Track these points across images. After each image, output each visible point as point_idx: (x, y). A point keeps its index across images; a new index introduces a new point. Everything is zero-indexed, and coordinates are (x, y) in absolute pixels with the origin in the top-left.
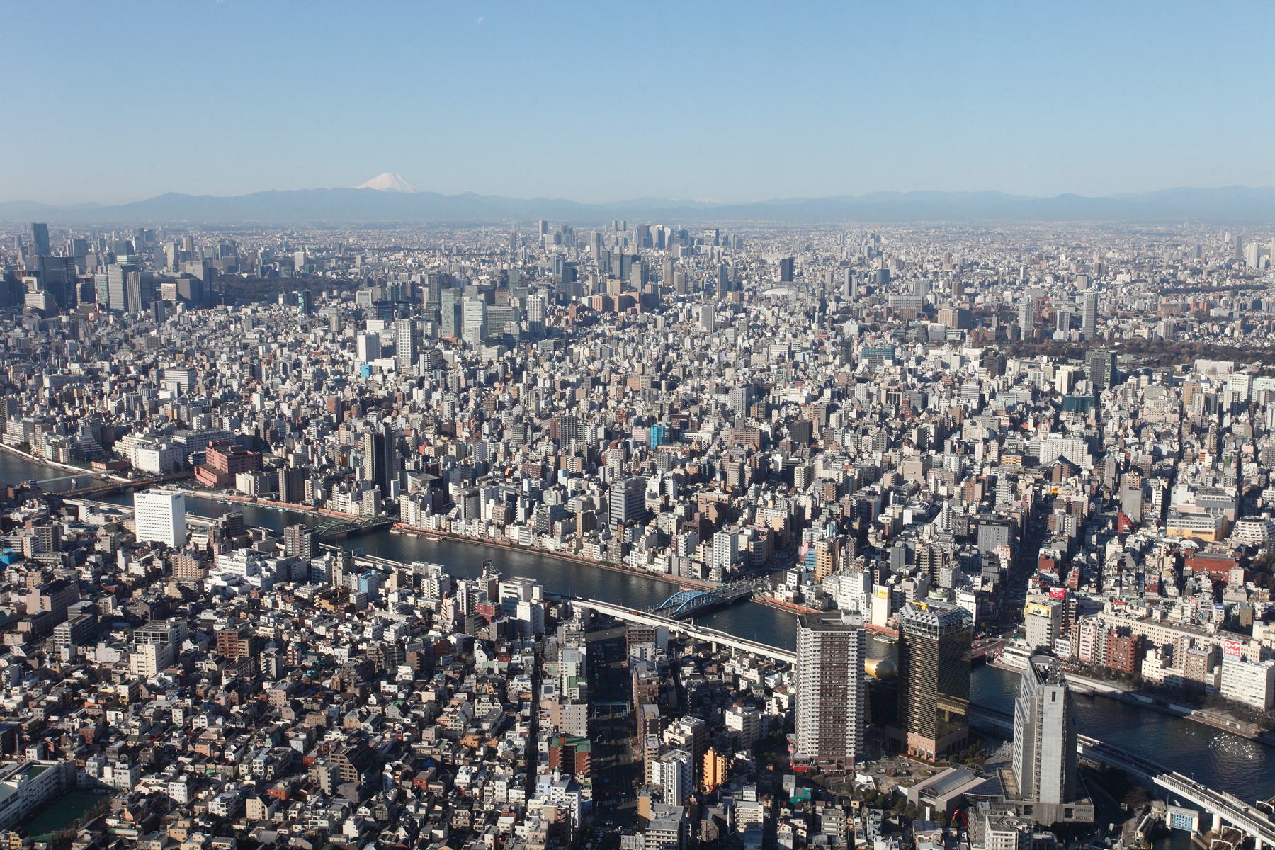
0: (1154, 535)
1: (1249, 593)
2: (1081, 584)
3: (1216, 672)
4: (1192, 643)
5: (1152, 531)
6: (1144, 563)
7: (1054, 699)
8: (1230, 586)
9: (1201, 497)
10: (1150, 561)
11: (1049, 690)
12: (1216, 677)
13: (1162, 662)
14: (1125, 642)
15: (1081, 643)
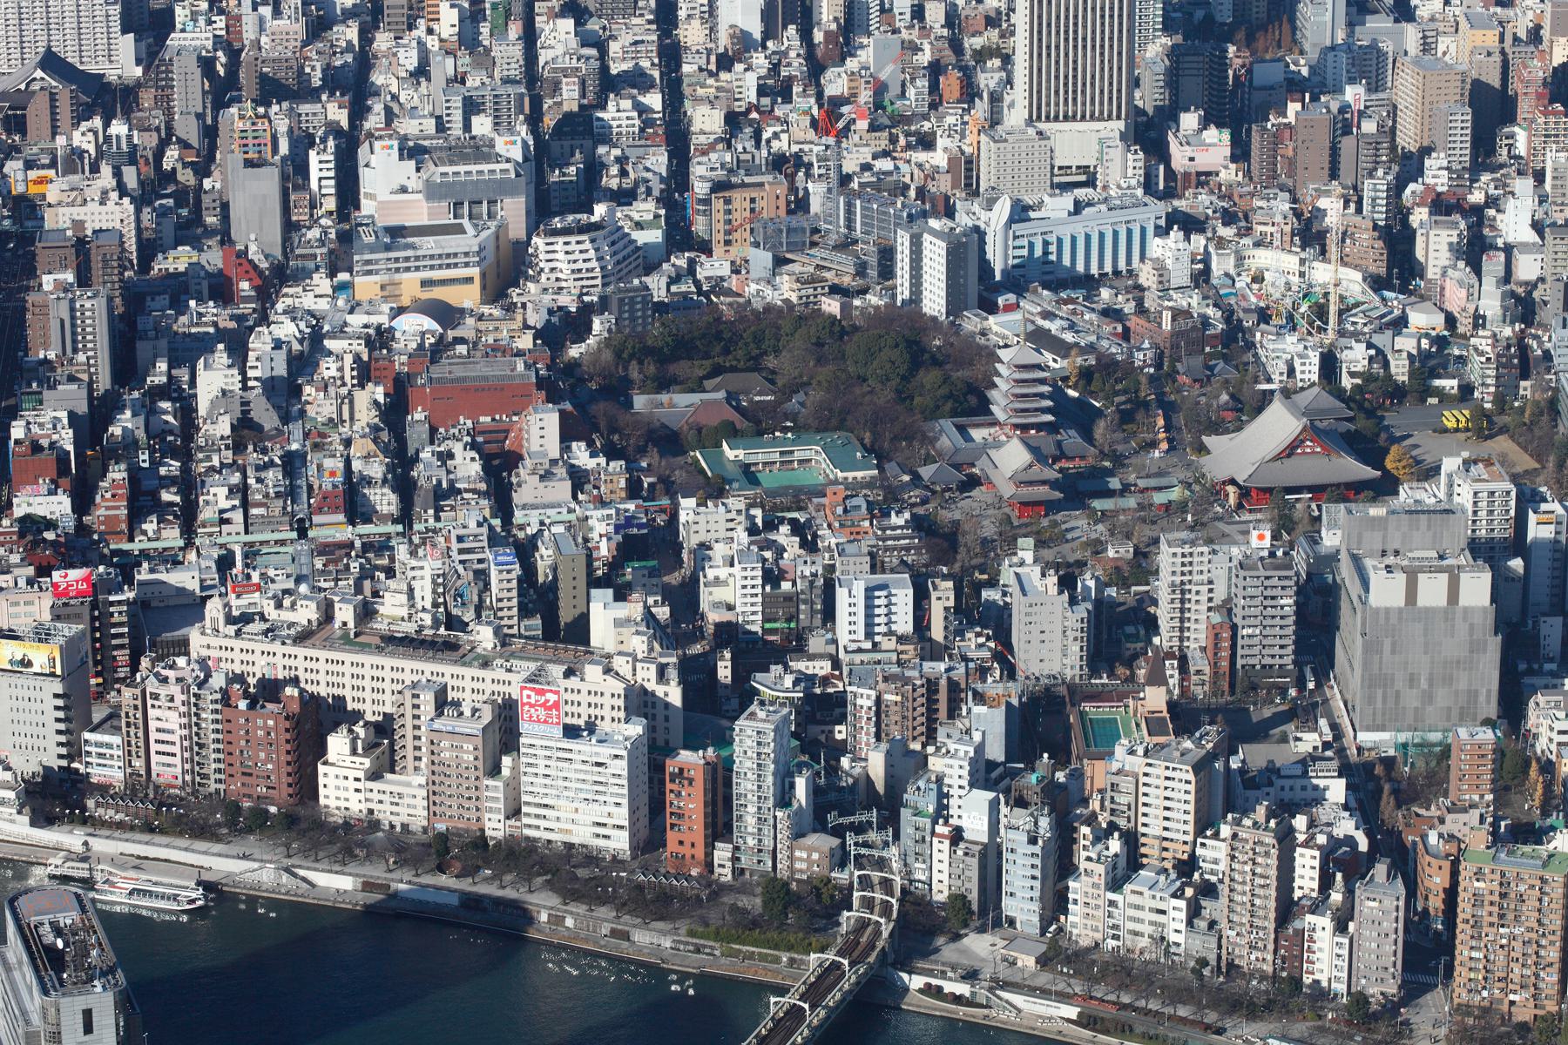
0: (323, 305)
1: (579, 479)
2: (136, 516)
3: (506, 772)
4: (442, 702)
5: (314, 295)
6: (302, 413)
7: (88, 1029)
8: (528, 462)
9: (435, 172)
10: (318, 405)
11: (71, 1007)
12: (507, 785)
13: (367, 762)
14: (269, 720)
15: (153, 736)
